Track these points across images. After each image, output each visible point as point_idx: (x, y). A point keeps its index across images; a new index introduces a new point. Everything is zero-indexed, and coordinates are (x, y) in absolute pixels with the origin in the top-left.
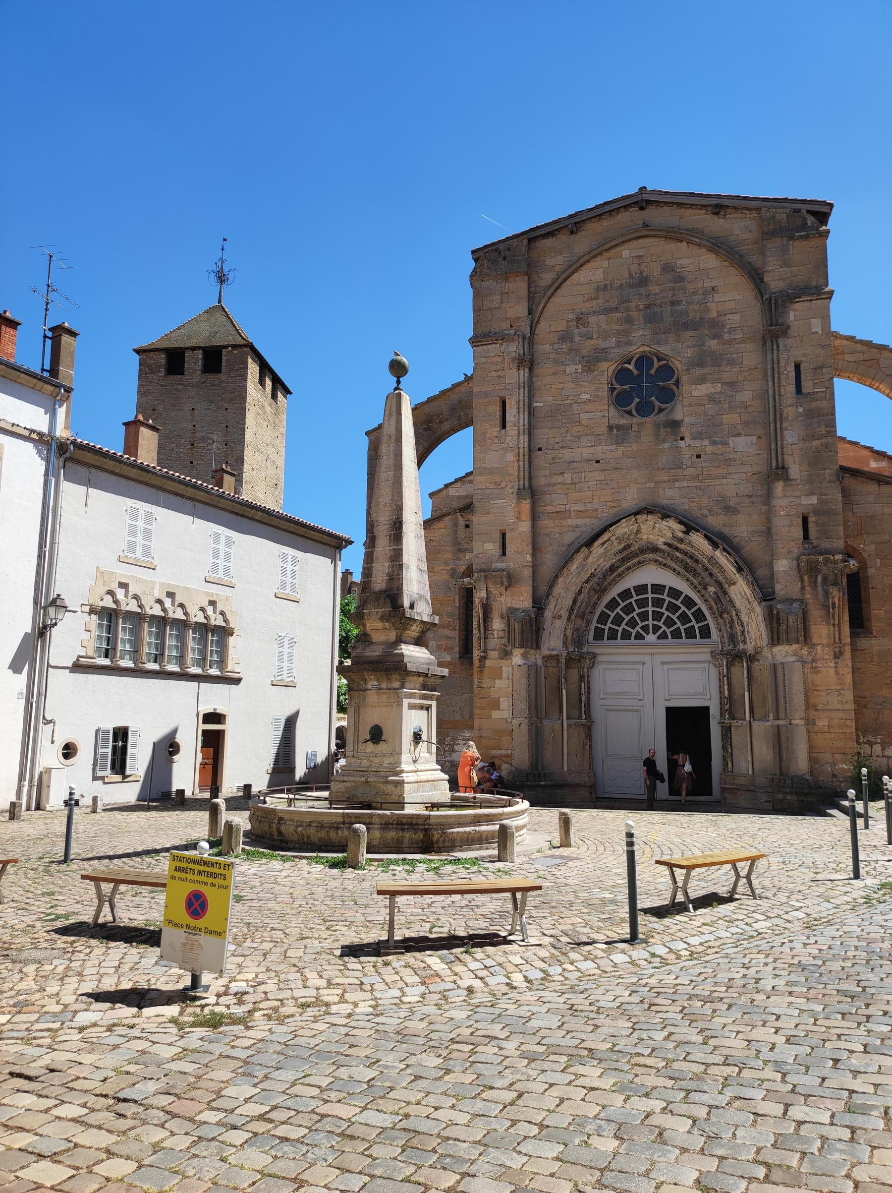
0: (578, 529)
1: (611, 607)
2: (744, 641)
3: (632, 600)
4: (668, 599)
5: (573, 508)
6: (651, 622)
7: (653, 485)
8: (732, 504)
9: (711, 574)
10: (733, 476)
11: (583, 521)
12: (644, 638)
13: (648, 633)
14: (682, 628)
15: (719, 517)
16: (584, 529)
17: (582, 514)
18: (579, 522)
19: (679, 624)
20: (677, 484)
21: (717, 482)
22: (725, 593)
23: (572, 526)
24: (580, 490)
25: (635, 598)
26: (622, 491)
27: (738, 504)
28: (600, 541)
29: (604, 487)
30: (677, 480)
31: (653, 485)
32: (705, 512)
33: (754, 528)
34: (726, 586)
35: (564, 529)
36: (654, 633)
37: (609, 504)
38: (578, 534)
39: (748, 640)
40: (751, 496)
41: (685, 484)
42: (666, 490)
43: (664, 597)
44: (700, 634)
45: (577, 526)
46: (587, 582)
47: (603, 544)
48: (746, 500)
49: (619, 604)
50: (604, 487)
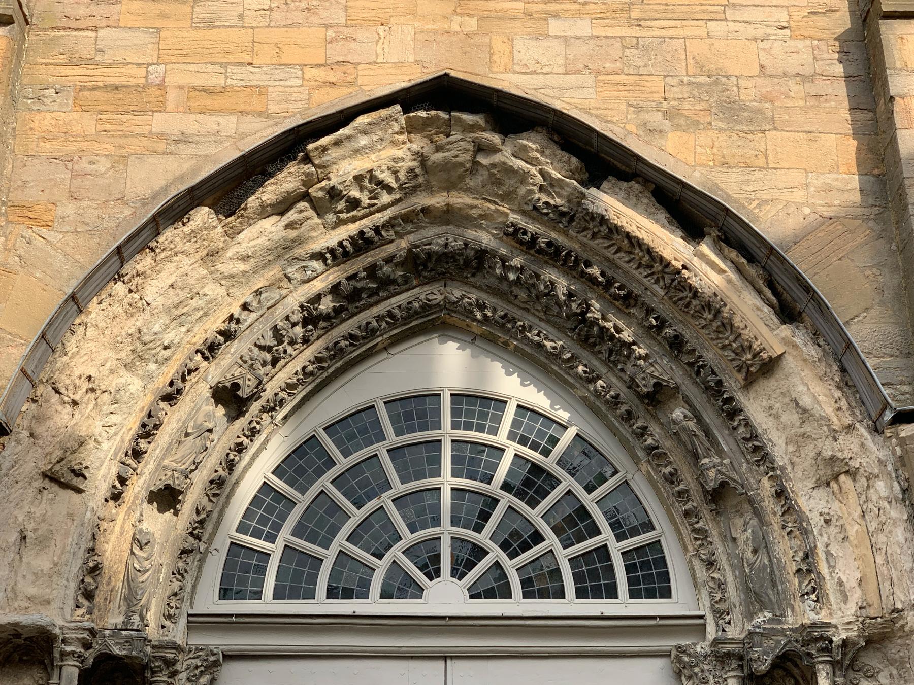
0: (189, 150)
1: (300, 471)
2: (816, 591)
3: (381, 449)
4: (512, 449)
5: (178, 76)
6: (446, 531)
7: (472, 24)
8: (748, 93)
9: (676, 345)
10: (747, 15)
11: (210, 123)
12: (418, 591)
13: (433, 573)
14: (563, 556)
15: (705, 138)
16: (212, 150)
17: (208, 102)
18: (191, 124)
19: (551, 540)
20: (555, 27)
21: (691, 28)
22: (731, 411)
23: (162, 136)
24: (209, 24)
25: (392, 439)
26: (360, 35)
27: (764, 98)
28: (269, 192)
29: (298, 17)
30: (556, 15)
31: (472, 24)
32: (656, 119)
33: (829, 178)
34: (733, 383)
35: (135, 145)
36: (458, 572)
37: (310, 73)
38: (186, 166)
39: (830, 586)
40: (809, 79)
41: (583, 27)
42: (519, 44)
43: (501, 438)
44: (631, 582)
45: (183, 139)
46: (210, 350)
47: (282, 207)
48: (795, 88)
49: (331, 463)
50: (298, 17)
